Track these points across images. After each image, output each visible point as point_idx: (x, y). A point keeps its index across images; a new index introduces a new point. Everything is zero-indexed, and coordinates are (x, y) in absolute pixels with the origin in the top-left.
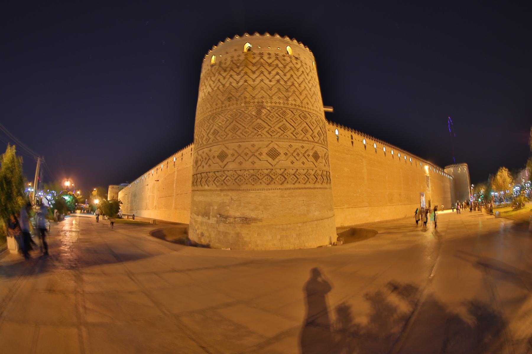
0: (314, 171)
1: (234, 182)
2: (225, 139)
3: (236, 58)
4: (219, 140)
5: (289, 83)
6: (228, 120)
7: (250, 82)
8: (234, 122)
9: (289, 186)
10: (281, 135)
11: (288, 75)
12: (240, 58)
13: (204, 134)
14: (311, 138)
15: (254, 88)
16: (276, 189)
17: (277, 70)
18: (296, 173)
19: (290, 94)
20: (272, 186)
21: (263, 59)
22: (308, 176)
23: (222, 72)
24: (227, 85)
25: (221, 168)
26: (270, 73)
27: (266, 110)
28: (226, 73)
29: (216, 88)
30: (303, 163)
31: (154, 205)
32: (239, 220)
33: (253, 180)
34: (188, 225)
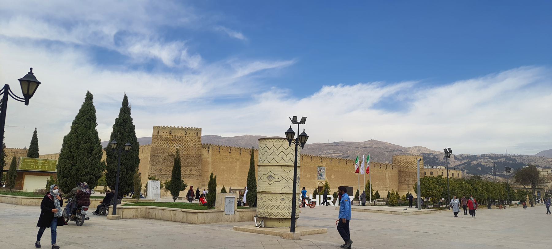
3: (166, 136)
5: (184, 147)
11: (184, 144)
15: (172, 149)
17: (180, 142)
24: (163, 146)
26: (177, 144)
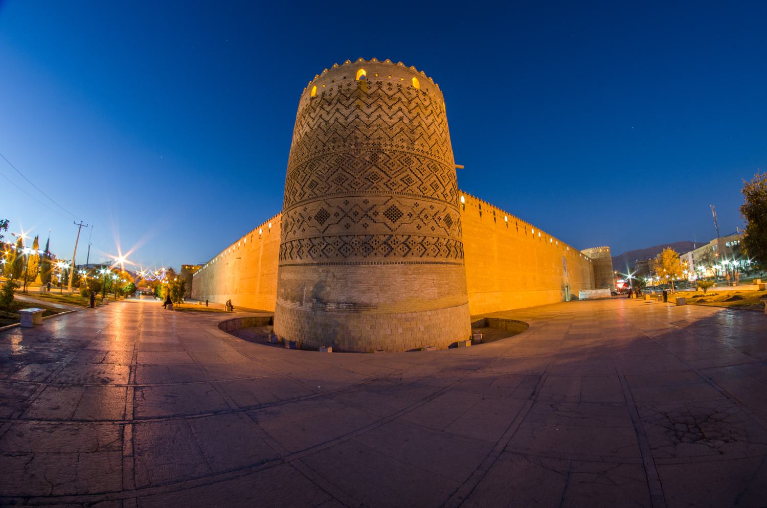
0: (447, 240)
1: (337, 252)
2: (326, 193)
3: (345, 87)
4: (318, 195)
5: (415, 123)
6: (332, 167)
7: (364, 118)
8: (340, 169)
9: (414, 259)
10: (404, 190)
11: (414, 113)
12: (350, 88)
13: (297, 188)
14: (442, 197)
15: (368, 126)
16: (396, 263)
17: (399, 105)
18: (424, 242)
19: (417, 137)
20: (391, 258)
21: (382, 90)
22: (439, 247)
23: (325, 106)
24: (332, 121)
25: (319, 233)
27: (384, 155)
28: (332, 106)
29: (316, 127)
30: (433, 229)
31: (235, 288)
32: (345, 306)
33: (364, 250)
34: (273, 313)
